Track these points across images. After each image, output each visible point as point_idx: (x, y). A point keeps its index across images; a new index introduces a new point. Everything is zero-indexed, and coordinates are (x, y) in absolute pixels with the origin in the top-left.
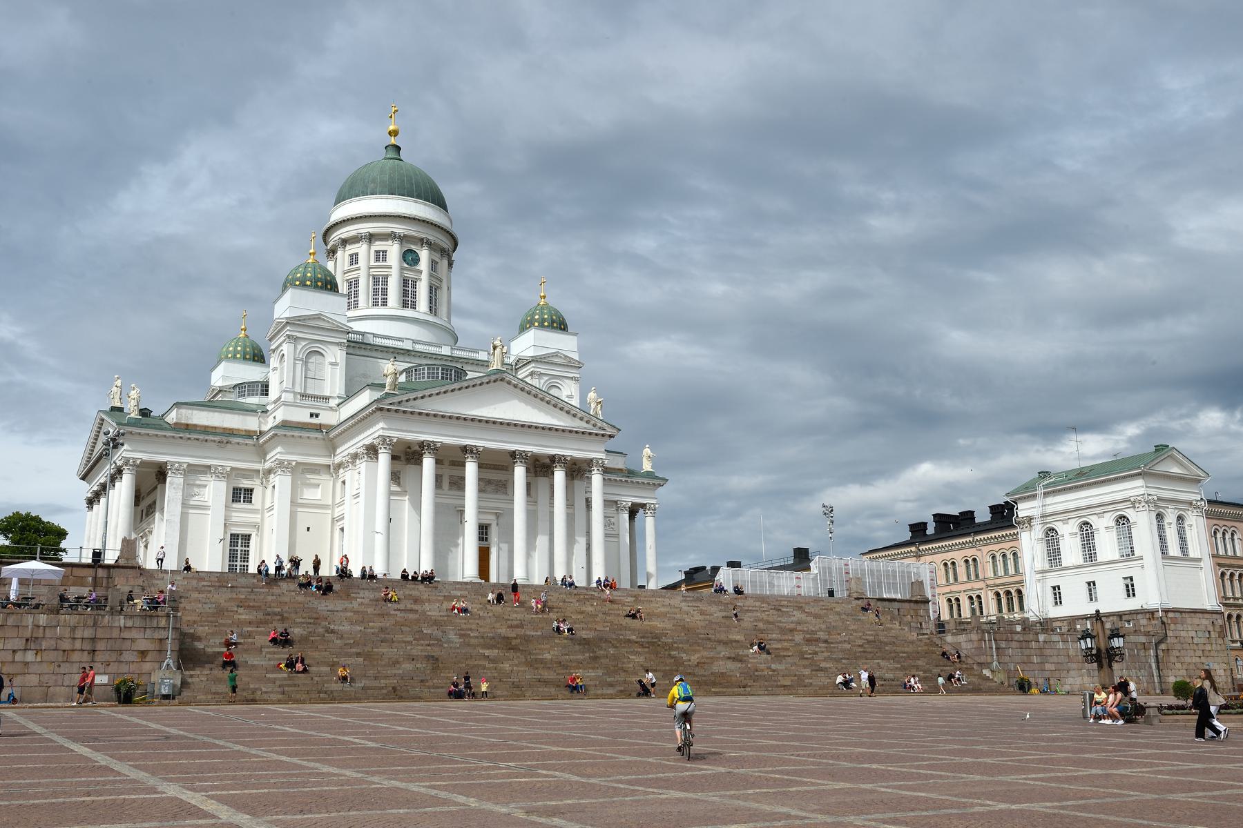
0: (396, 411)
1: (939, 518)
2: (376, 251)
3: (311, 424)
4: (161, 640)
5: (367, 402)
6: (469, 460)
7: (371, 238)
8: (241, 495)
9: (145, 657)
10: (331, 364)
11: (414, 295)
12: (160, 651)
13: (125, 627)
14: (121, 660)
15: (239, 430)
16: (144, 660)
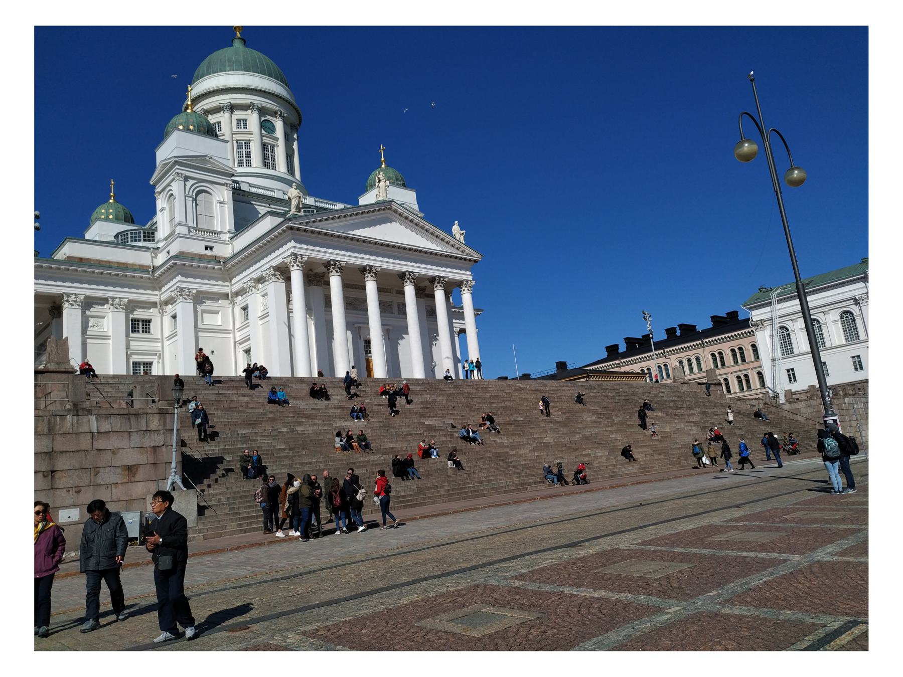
0: (305, 230)
1: (629, 341)
2: (237, 120)
3: (207, 256)
4: (154, 448)
5: (270, 227)
6: (369, 278)
7: (232, 108)
8: (139, 326)
9: (134, 476)
10: (220, 203)
11: (273, 159)
12: (155, 464)
13: (99, 432)
14: (99, 481)
15: (133, 265)
16: (133, 479)
